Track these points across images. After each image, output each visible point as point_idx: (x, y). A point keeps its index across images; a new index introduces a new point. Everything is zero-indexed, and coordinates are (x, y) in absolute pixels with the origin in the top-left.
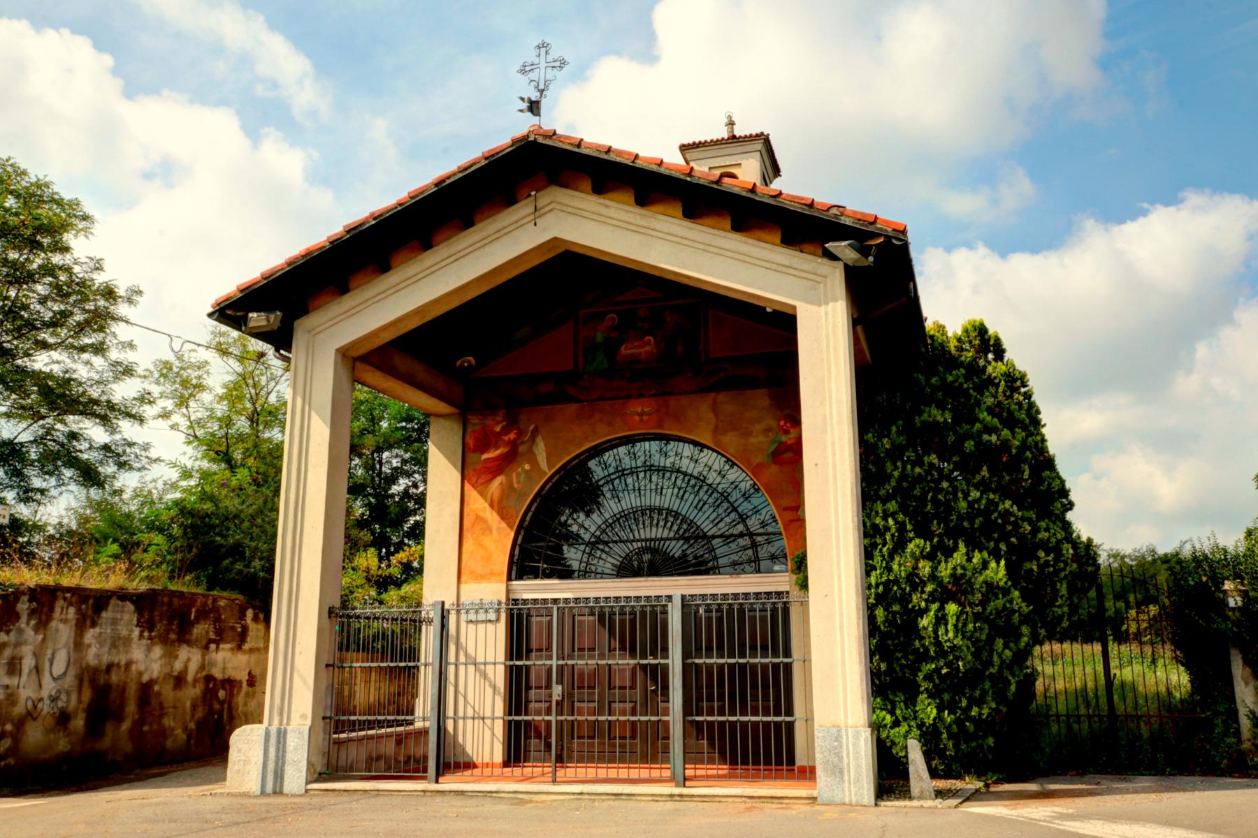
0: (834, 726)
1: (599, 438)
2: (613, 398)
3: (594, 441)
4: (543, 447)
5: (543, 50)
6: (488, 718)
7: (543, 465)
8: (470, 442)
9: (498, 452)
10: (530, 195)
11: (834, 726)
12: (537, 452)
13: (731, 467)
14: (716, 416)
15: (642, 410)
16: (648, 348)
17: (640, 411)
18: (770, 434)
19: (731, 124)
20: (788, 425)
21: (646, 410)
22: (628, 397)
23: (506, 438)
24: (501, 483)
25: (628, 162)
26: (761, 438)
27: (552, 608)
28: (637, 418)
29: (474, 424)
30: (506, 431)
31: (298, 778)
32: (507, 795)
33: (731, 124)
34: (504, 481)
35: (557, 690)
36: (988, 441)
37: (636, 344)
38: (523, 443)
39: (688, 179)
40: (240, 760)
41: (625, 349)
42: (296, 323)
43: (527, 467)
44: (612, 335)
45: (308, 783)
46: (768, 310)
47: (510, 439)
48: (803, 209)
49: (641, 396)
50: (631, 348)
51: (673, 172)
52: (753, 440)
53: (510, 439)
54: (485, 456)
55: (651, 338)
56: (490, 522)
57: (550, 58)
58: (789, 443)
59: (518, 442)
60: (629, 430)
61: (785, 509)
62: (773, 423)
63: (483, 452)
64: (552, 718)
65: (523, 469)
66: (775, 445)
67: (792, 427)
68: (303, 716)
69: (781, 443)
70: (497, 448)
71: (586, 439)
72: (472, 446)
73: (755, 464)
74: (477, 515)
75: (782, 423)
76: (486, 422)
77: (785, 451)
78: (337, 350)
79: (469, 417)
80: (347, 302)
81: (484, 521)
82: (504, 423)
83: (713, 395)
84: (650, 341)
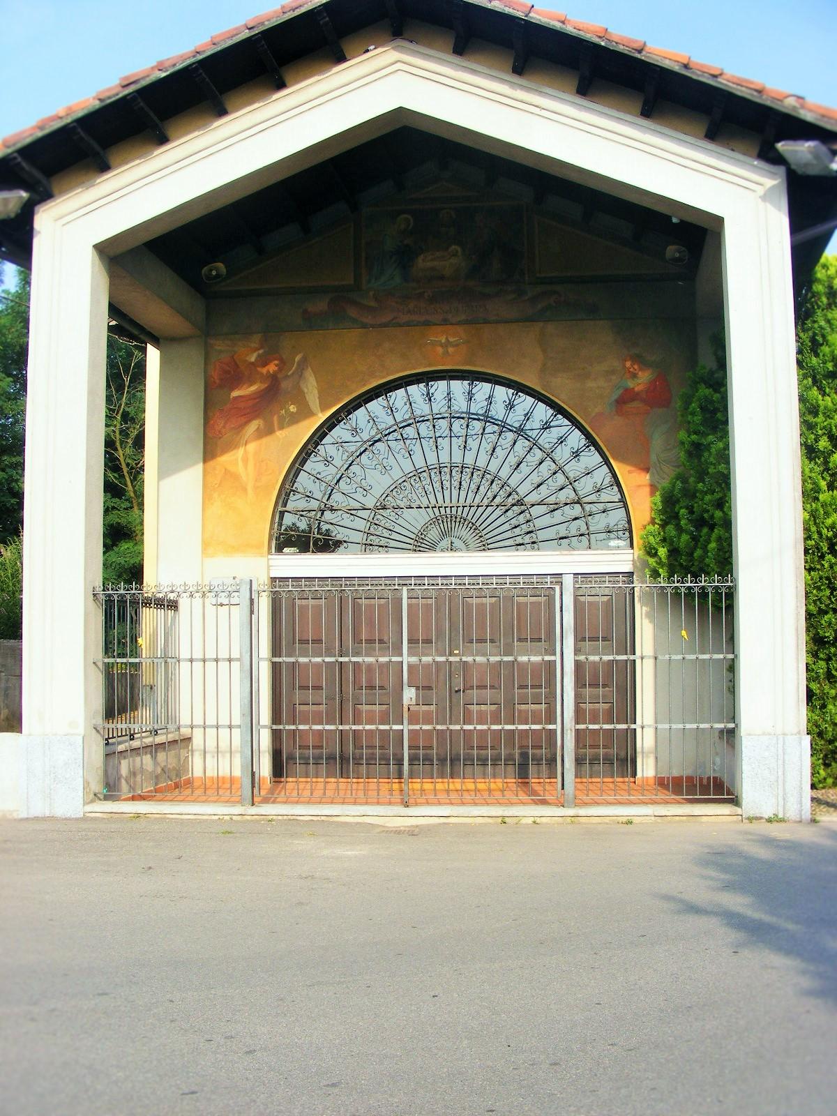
0: (764, 734)
1: (388, 375)
2: (408, 324)
3: (384, 377)
6: (224, 726)
8: (216, 375)
9: (253, 388)
11: (764, 734)
12: (306, 390)
14: (544, 351)
15: (447, 339)
16: (454, 261)
17: (443, 341)
18: (614, 377)
20: (636, 367)
21: (451, 340)
22: (427, 324)
23: (264, 371)
24: (258, 428)
25: (520, 15)
26: (602, 382)
28: (440, 350)
29: (220, 352)
30: (265, 364)
34: (262, 426)
35: (409, 695)
37: (438, 254)
38: (287, 377)
39: (603, 44)
41: (423, 260)
42: (36, 208)
43: (293, 408)
44: (406, 242)
45: (85, 804)
46: (675, 220)
47: (268, 371)
48: (752, 95)
49: (445, 322)
50: (432, 260)
51: (581, 33)
52: (590, 384)
53: (268, 371)
54: (235, 394)
55: (459, 249)
56: (244, 478)
59: (280, 376)
60: (430, 365)
62: (616, 364)
63: (232, 389)
64: (406, 727)
66: (620, 392)
67: (641, 369)
69: (627, 390)
70: (251, 385)
71: (372, 375)
72: (217, 381)
73: (593, 415)
74: (226, 469)
75: (628, 364)
76: (236, 349)
77: (633, 400)
79: (212, 342)
81: (235, 477)
82: (261, 351)
83: (541, 324)
84: (457, 251)
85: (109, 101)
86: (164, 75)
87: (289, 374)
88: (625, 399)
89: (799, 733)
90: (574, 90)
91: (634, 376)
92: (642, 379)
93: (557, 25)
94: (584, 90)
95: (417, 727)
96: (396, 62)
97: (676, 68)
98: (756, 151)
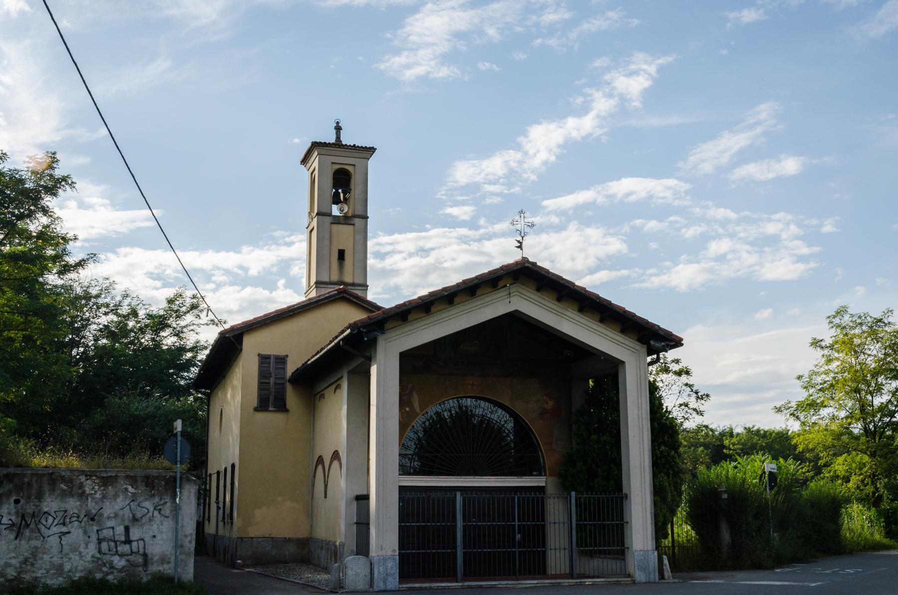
4: (417, 398)
5: (522, 215)
7: (417, 409)
10: (506, 286)
11: (641, 551)
12: (413, 401)
13: (444, 404)
17: (471, 383)
19: (338, 129)
20: (548, 399)
21: (475, 383)
27: (515, 497)
28: (470, 387)
31: (394, 582)
32: (503, 586)
33: (338, 129)
35: (518, 537)
36: (664, 423)
40: (353, 575)
43: (407, 409)
55: (477, 342)
57: (526, 220)
58: (549, 408)
61: (546, 444)
64: (517, 550)
65: (405, 410)
67: (550, 400)
68: (394, 551)
75: (545, 398)
78: (401, 354)
80: (407, 328)
85: (425, 301)
86: (446, 294)
87: (407, 393)
88: (543, 412)
89: (653, 550)
90: (577, 310)
91: (547, 403)
92: (550, 405)
93: (584, 292)
94: (581, 310)
95: (521, 550)
96: (516, 291)
97: (621, 312)
98: (636, 338)
